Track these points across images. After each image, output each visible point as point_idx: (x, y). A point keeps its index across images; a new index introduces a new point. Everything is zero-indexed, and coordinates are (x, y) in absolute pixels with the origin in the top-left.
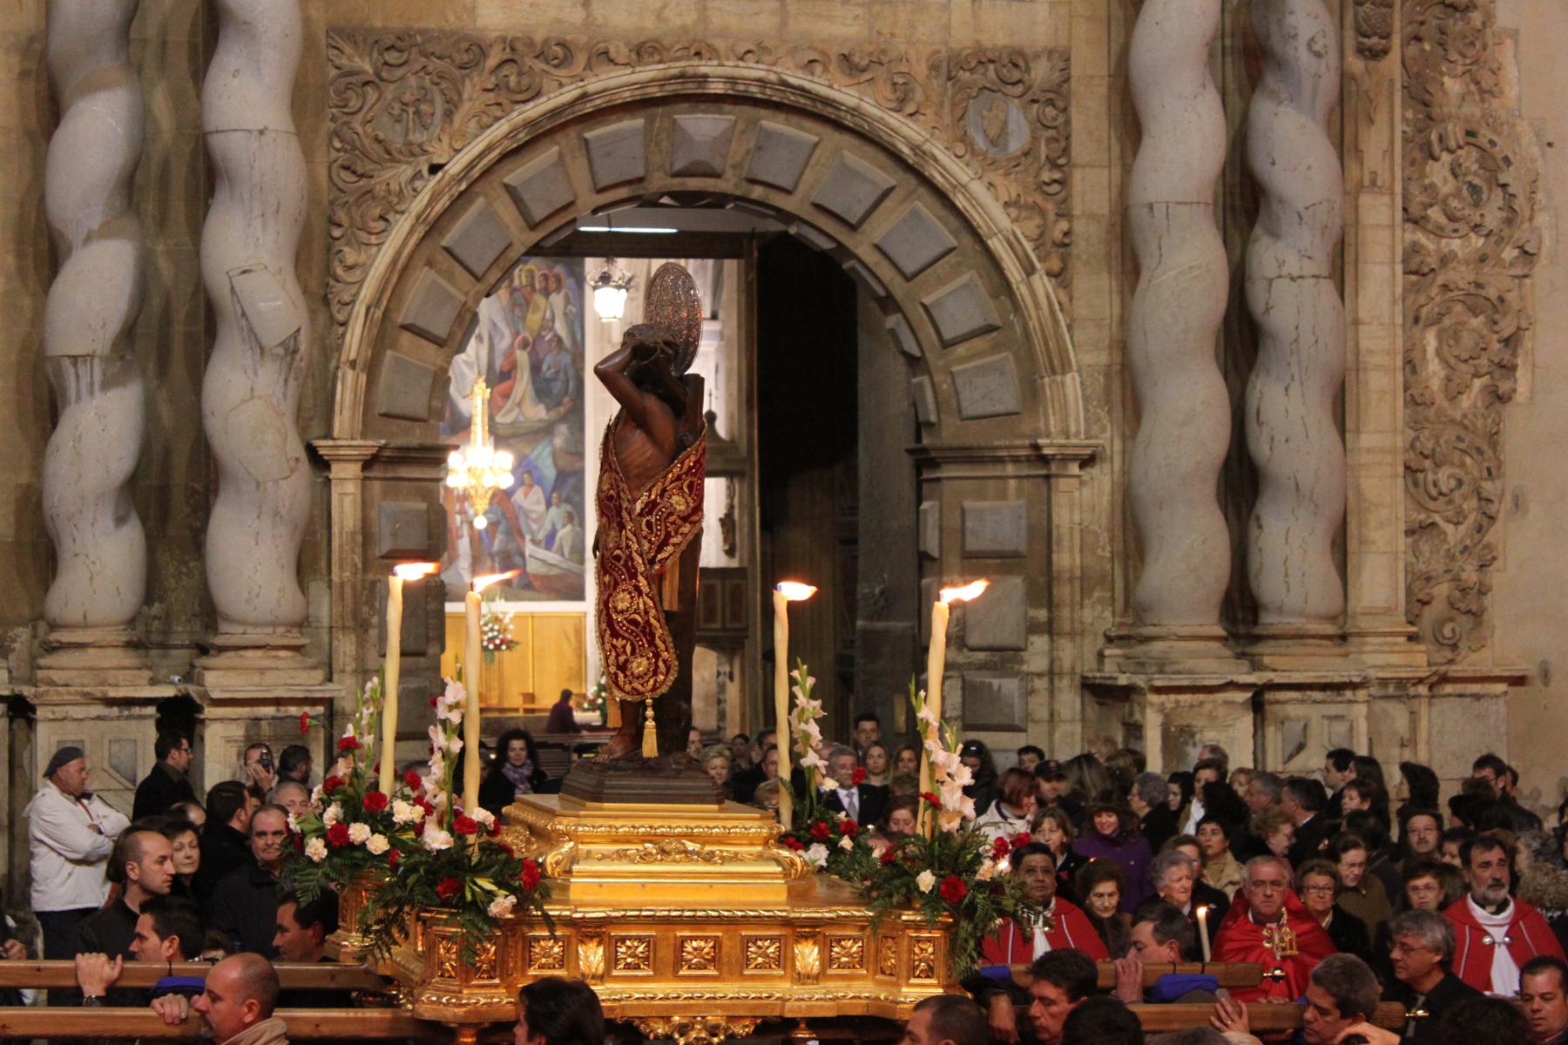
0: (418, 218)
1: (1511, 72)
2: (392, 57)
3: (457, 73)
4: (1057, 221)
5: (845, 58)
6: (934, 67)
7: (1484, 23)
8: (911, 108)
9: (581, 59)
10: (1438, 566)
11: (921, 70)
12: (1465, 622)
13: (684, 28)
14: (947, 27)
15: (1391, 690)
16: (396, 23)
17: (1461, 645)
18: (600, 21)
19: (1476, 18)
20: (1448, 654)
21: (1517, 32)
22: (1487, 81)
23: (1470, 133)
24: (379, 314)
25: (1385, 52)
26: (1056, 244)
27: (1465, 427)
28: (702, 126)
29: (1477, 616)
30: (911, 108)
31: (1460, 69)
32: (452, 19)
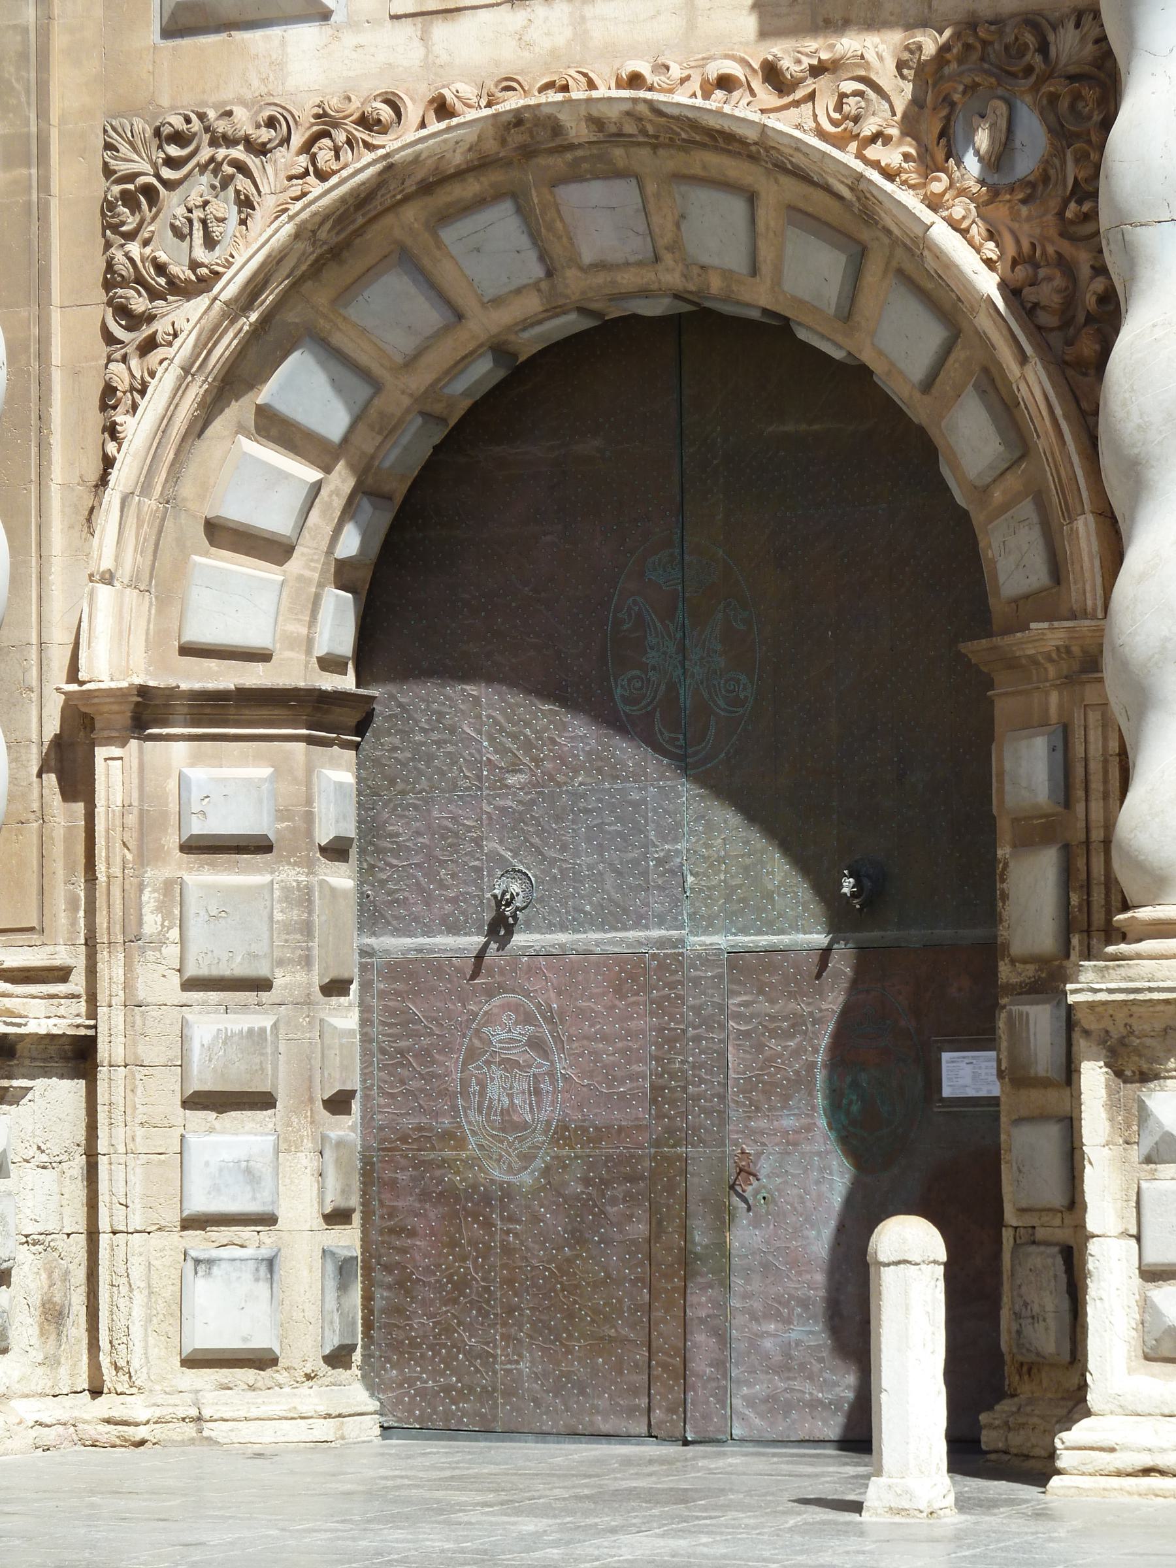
0: (186, 370)
3: (252, 161)
4: (1092, 278)
13: (553, 53)
16: (189, 101)
18: (444, 58)
24: (151, 504)
26: (1090, 319)
32: (256, 83)
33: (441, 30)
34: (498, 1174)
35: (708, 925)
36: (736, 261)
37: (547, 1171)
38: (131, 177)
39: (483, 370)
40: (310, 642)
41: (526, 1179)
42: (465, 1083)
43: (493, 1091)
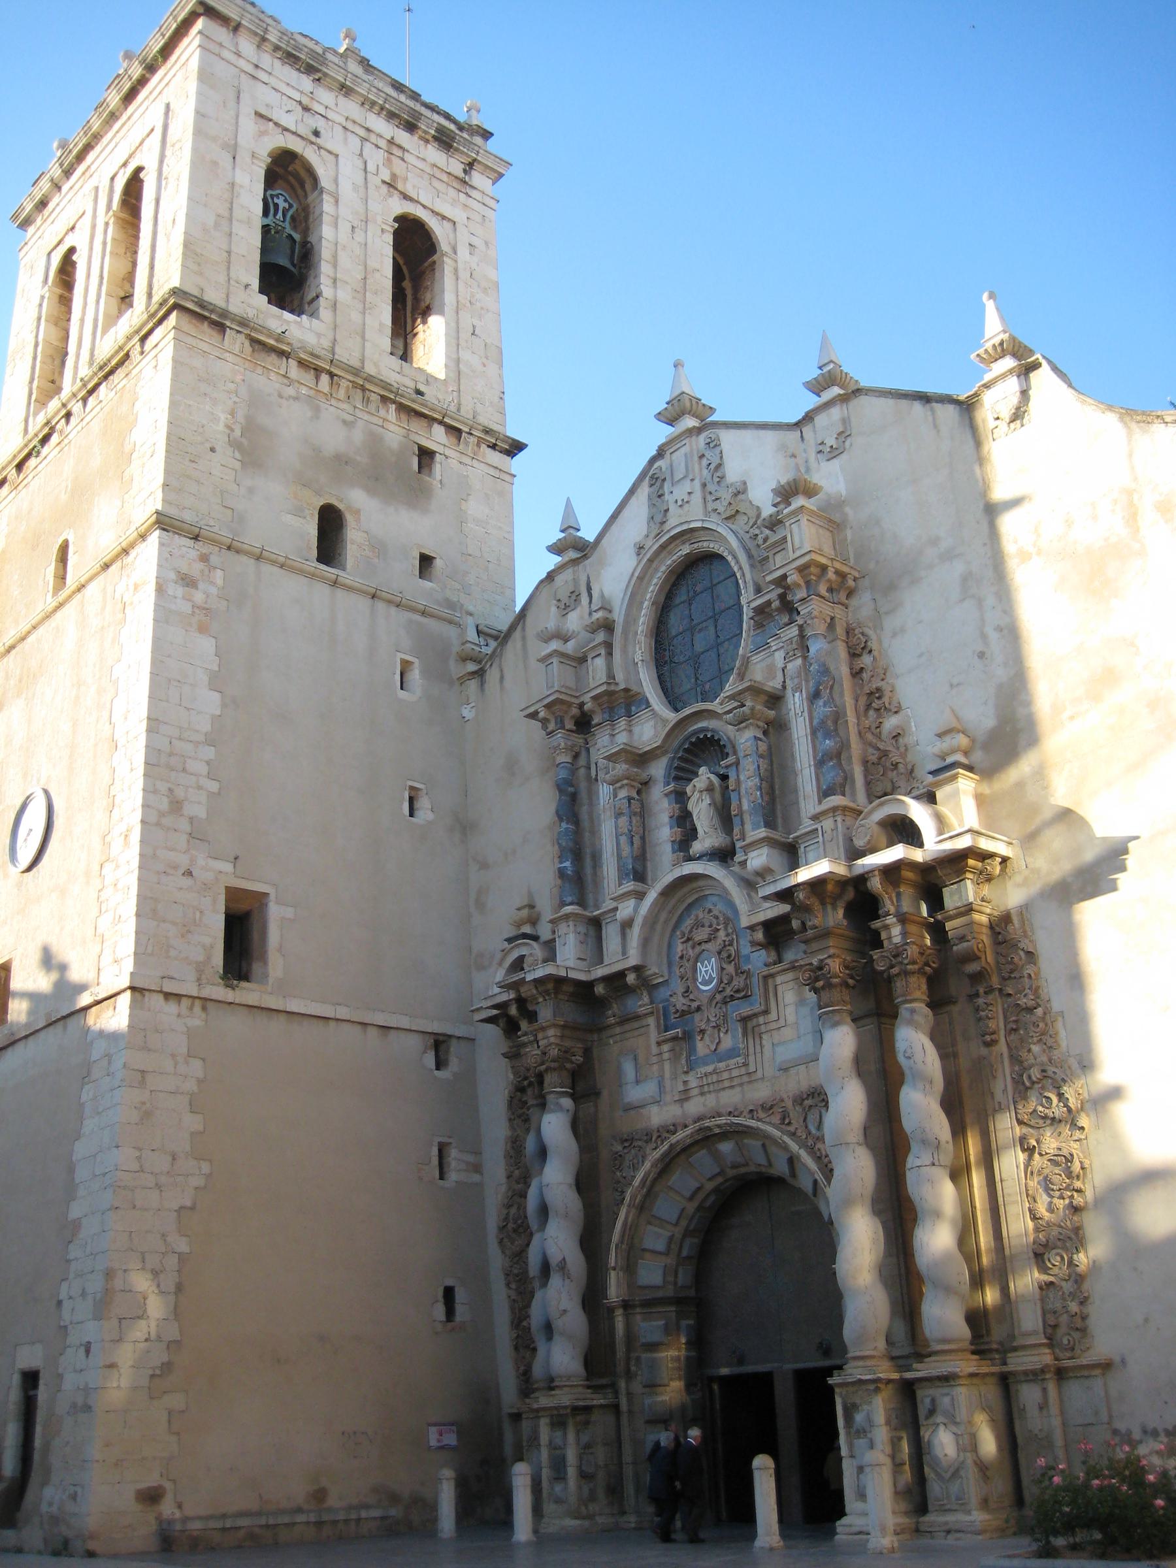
1: (1062, 1034)
2: (626, 1144)
5: (762, 1106)
6: (794, 1101)
7: (1045, 1013)
8: (787, 1121)
9: (679, 1128)
10: (1058, 1305)
11: (789, 1104)
12: (1076, 1335)
14: (799, 1082)
15: (1031, 1377)
17: (1076, 1348)
19: (1039, 1011)
20: (1068, 1354)
21: (1062, 1012)
22: (1050, 1042)
23: (1044, 1071)
25: (994, 1042)
27: (1061, 1227)
28: (726, 1147)
29: (1083, 1331)
30: (787, 1121)
31: (1035, 1039)
33: (687, 1105)
36: (764, 1162)
38: (617, 1153)
39: (712, 1198)
40: (675, 1283)
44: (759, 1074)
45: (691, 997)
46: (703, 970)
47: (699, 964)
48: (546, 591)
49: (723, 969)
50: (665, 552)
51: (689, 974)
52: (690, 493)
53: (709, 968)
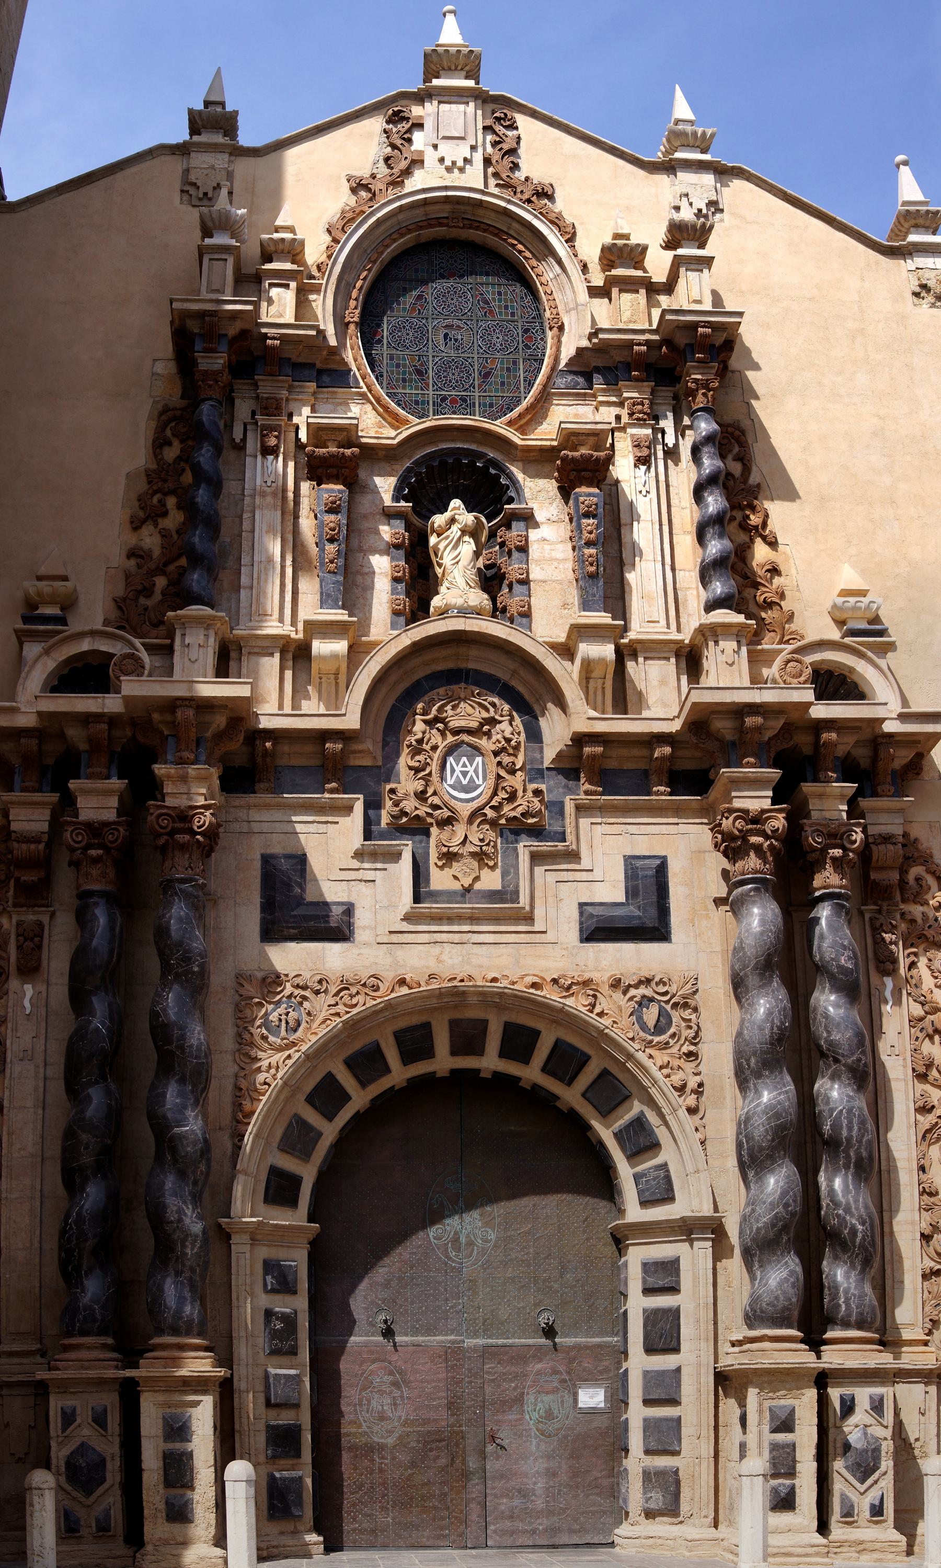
34: (376, 1439)
35: (475, 1335)
37: (400, 1437)
41: (390, 1441)
42: (361, 1401)
43: (374, 1403)
44: (549, 937)
45: (436, 800)
46: (458, 769)
47: (451, 760)
48: (175, 165)
49: (499, 777)
50: (422, 209)
51: (434, 767)
52: (465, 160)
53: (470, 769)
